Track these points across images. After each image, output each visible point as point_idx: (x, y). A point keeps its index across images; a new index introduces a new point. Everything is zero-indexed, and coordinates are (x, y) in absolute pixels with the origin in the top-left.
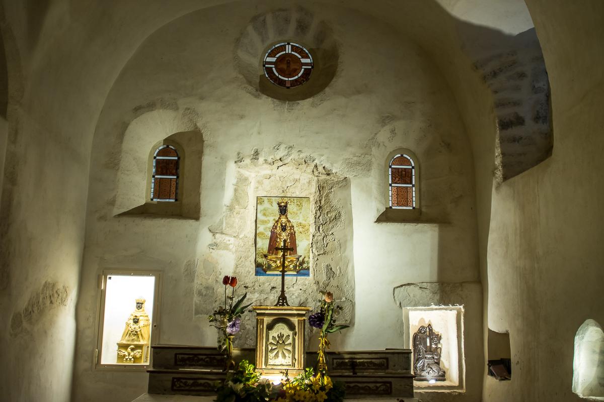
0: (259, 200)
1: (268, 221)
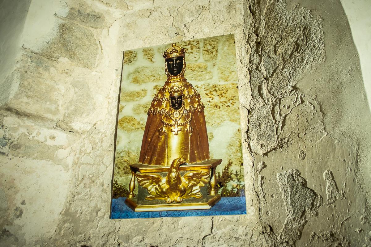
0: (129, 57)
1: (143, 92)
